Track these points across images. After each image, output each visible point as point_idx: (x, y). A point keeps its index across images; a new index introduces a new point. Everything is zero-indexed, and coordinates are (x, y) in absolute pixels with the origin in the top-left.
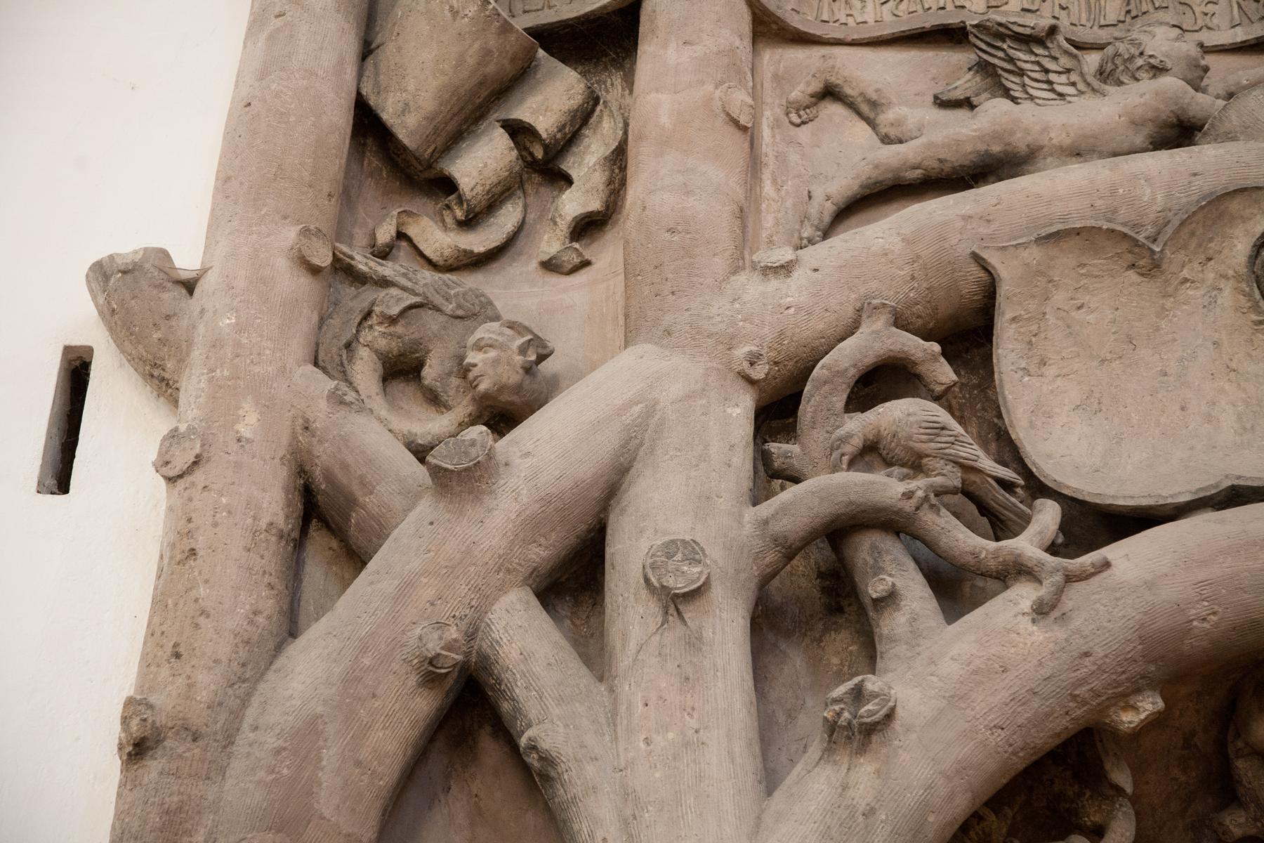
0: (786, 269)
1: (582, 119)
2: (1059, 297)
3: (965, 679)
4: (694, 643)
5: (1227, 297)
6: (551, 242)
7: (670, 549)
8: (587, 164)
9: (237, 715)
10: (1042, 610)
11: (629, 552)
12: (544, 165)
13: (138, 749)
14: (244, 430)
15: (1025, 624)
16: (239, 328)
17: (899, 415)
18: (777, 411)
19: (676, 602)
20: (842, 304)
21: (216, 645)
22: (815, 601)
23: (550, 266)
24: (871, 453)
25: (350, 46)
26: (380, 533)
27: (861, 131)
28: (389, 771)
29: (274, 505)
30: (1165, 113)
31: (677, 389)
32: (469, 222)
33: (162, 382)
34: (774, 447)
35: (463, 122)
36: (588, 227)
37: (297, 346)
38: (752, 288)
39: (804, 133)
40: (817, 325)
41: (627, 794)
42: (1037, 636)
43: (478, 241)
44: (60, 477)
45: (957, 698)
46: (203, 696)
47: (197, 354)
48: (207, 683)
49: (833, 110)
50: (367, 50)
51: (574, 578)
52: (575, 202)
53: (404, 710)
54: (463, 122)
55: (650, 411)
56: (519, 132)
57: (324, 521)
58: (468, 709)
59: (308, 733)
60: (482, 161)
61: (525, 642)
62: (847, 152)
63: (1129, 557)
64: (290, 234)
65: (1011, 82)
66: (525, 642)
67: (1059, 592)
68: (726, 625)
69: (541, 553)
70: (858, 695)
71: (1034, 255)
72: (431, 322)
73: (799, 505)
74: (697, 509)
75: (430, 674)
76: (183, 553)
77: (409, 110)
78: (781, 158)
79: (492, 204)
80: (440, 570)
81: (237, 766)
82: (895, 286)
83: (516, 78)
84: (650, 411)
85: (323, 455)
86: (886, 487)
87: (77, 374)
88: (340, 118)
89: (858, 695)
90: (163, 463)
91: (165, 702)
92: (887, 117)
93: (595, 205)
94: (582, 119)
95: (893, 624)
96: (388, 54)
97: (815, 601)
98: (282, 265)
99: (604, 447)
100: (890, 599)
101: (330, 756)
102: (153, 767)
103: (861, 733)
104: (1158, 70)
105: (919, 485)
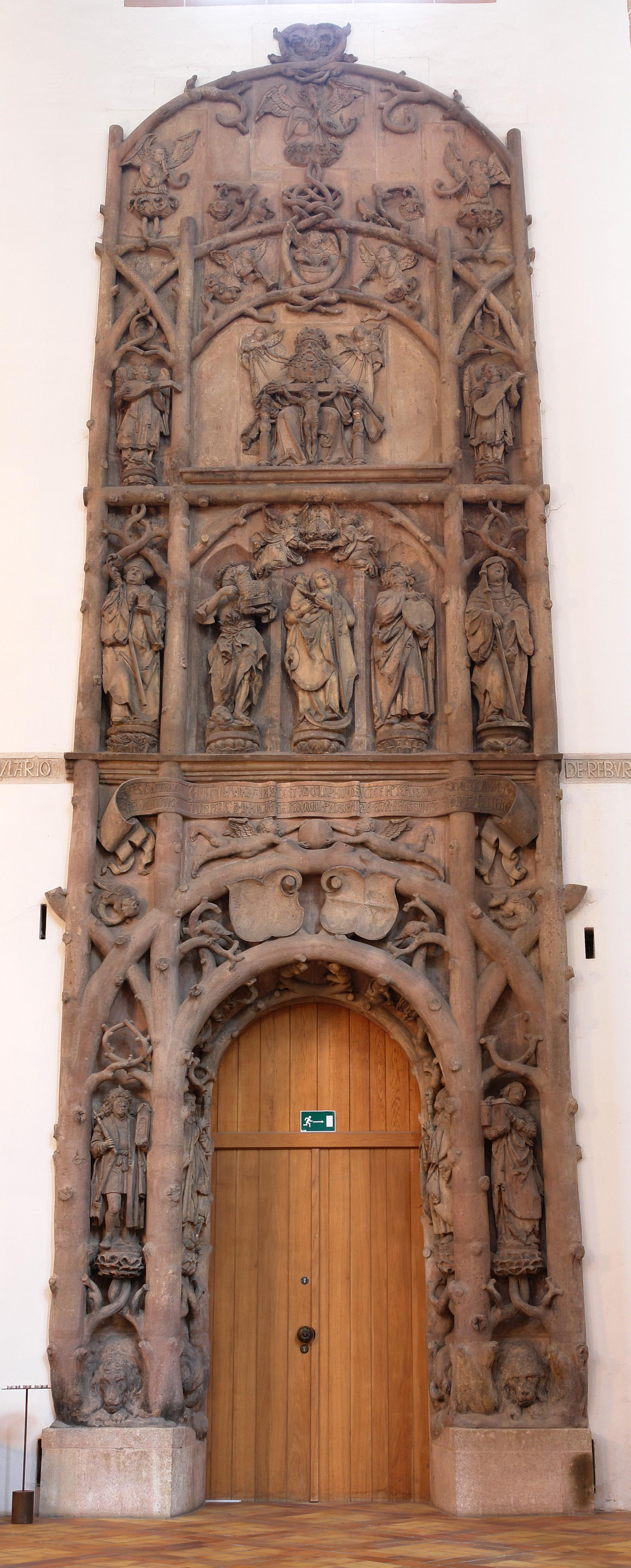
0: (186, 891)
1: (144, 841)
2: (243, 892)
3: (217, 981)
4: (166, 978)
5: (277, 889)
6: (140, 868)
7: (161, 960)
8: (148, 848)
9: (82, 994)
10: (231, 969)
11: (155, 957)
12: (137, 849)
13: (65, 1002)
14: (79, 933)
15: (228, 971)
16: (76, 909)
17: (207, 924)
18: (185, 918)
19: (162, 971)
20: (197, 898)
21: (77, 981)
22: (191, 963)
23: (141, 874)
24: (203, 932)
25: (95, 828)
26: (107, 953)
27: (206, 843)
28: (110, 1004)
29: (85, 948)
30: (269, 842)
31: (162, 922)
32: (123, 863)
33: (61, 915)
34: (184, 929)
35: (119, 843)
36: (148, 865)
37: (88, 911)
38: (180, 896)
39: (194, 844)
40: (192, 904)
41: (154, 1008)
42: (229, 974)
43: (124, 868)
44: (43, 937)
45: (214, 987)
46: (76, 992)
47: (68, 915)
48: (77, 989)
49: (200, 837)
50: (98, 827)
51: (145, 957)
52: (145, 859)
53: (112, 991)
54: (119, 843)
55: (158, 926)
56: (131, 843)
57: (96, 949)
58: (125, 988)
59: (95, 999)
60: (124, 851)
61: (135, 976)
62: (202, 849)
63: (249, 955)
64: (84, 886)
65: (238, 833)
66: (135, 976)
67: (234, 965)
68: (173, 974)
69: (137, 957)
70: (195, 988)
71: (237, 885)
72: (114, 898)
73: (188, 944)
74: (166, 951)
75: (117, 985)
76: (69, 962)
77: (107, 844)
78: (189, 850)
79: (127, 859)
80: (119, 964)
81: (83, 1004)
82: (209, 893)
83: (132, 830)
84: (158, 926)
85: (95, 937)
86: (205, 940)
87: (44, 909)
88: (92, 847)
89: (195, 988)
90: (64, 940)
91: (70, 992)
92: (212, 840)
93: (149, 861)
94: (144, 841)
95: (205, 969)
96: (102, 829)
97: (191, 963)
98: (83, 893)
99: (149, 934)
100: (205, 963)
101: (100, 1003)
102: (69, 1005)
103: (194, 997)
104: (268, 832)
105: (211, 939)
